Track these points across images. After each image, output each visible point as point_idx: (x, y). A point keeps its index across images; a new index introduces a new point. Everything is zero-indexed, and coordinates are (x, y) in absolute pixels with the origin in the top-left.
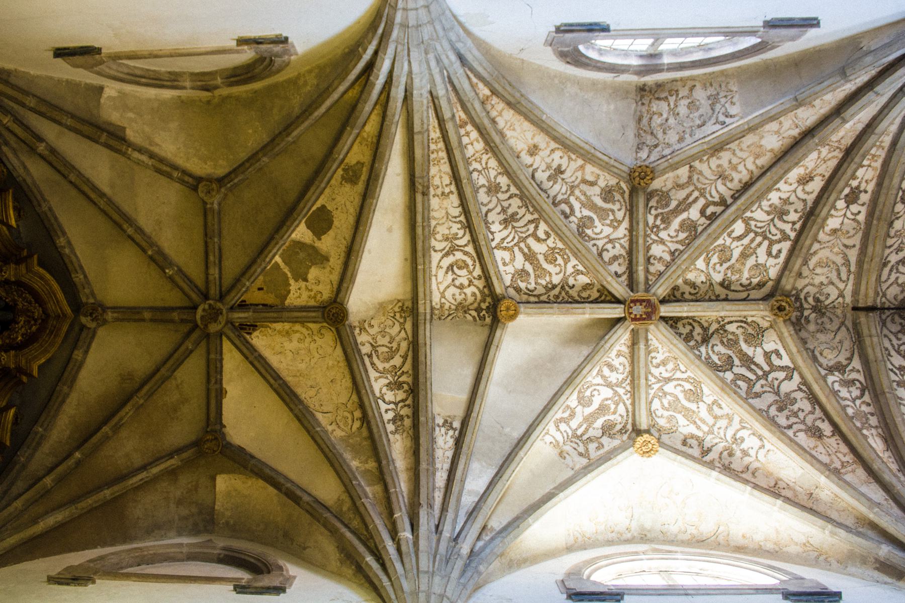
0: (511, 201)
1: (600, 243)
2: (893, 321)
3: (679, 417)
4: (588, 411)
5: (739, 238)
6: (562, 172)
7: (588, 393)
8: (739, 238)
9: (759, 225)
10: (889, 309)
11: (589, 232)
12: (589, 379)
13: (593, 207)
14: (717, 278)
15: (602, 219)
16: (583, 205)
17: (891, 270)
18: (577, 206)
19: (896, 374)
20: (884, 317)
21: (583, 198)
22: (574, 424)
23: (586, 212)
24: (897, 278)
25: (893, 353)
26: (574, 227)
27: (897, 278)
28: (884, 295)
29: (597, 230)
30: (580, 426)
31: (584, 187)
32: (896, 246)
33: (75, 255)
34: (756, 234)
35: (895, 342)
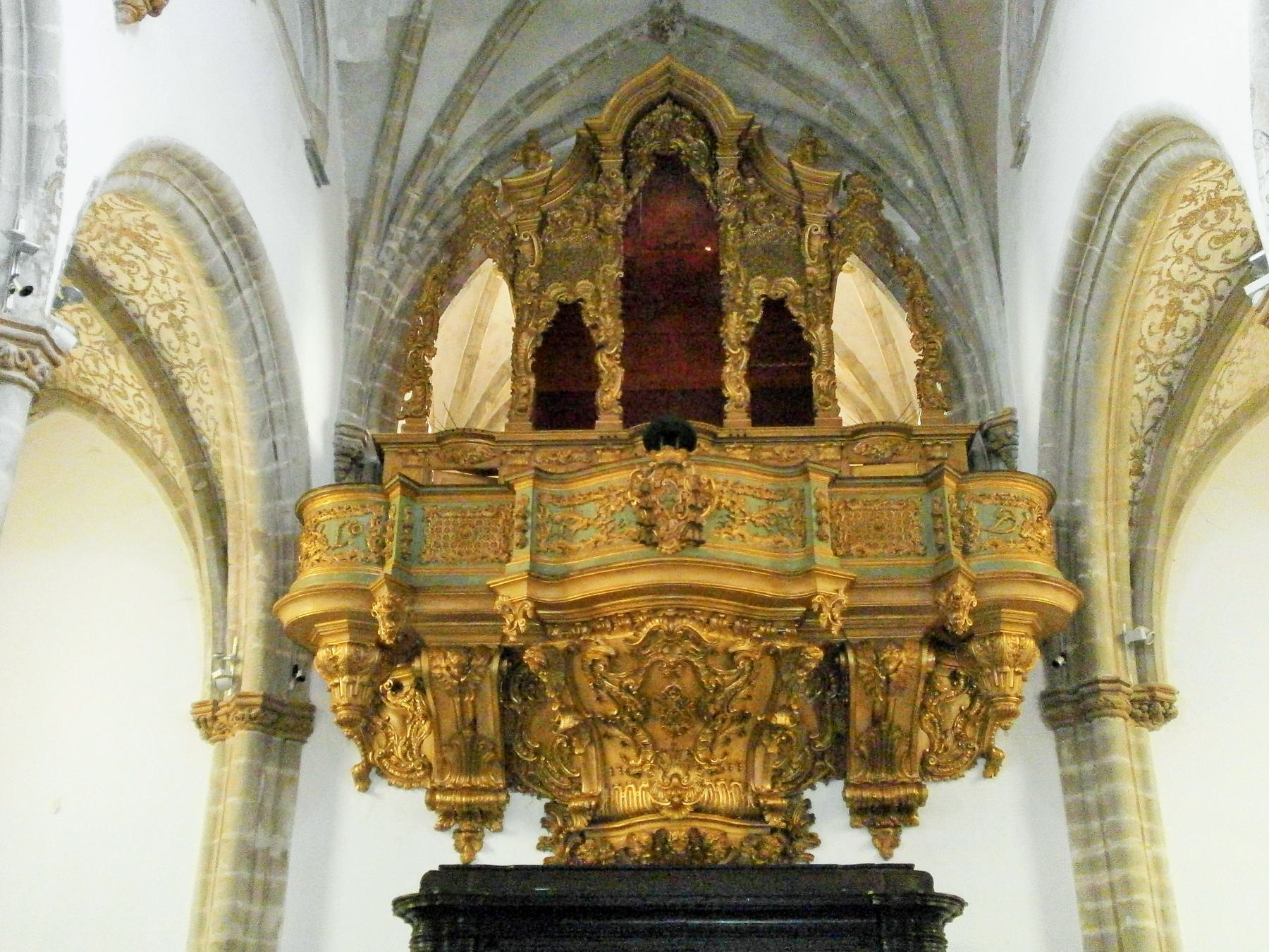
33: (580, 53)
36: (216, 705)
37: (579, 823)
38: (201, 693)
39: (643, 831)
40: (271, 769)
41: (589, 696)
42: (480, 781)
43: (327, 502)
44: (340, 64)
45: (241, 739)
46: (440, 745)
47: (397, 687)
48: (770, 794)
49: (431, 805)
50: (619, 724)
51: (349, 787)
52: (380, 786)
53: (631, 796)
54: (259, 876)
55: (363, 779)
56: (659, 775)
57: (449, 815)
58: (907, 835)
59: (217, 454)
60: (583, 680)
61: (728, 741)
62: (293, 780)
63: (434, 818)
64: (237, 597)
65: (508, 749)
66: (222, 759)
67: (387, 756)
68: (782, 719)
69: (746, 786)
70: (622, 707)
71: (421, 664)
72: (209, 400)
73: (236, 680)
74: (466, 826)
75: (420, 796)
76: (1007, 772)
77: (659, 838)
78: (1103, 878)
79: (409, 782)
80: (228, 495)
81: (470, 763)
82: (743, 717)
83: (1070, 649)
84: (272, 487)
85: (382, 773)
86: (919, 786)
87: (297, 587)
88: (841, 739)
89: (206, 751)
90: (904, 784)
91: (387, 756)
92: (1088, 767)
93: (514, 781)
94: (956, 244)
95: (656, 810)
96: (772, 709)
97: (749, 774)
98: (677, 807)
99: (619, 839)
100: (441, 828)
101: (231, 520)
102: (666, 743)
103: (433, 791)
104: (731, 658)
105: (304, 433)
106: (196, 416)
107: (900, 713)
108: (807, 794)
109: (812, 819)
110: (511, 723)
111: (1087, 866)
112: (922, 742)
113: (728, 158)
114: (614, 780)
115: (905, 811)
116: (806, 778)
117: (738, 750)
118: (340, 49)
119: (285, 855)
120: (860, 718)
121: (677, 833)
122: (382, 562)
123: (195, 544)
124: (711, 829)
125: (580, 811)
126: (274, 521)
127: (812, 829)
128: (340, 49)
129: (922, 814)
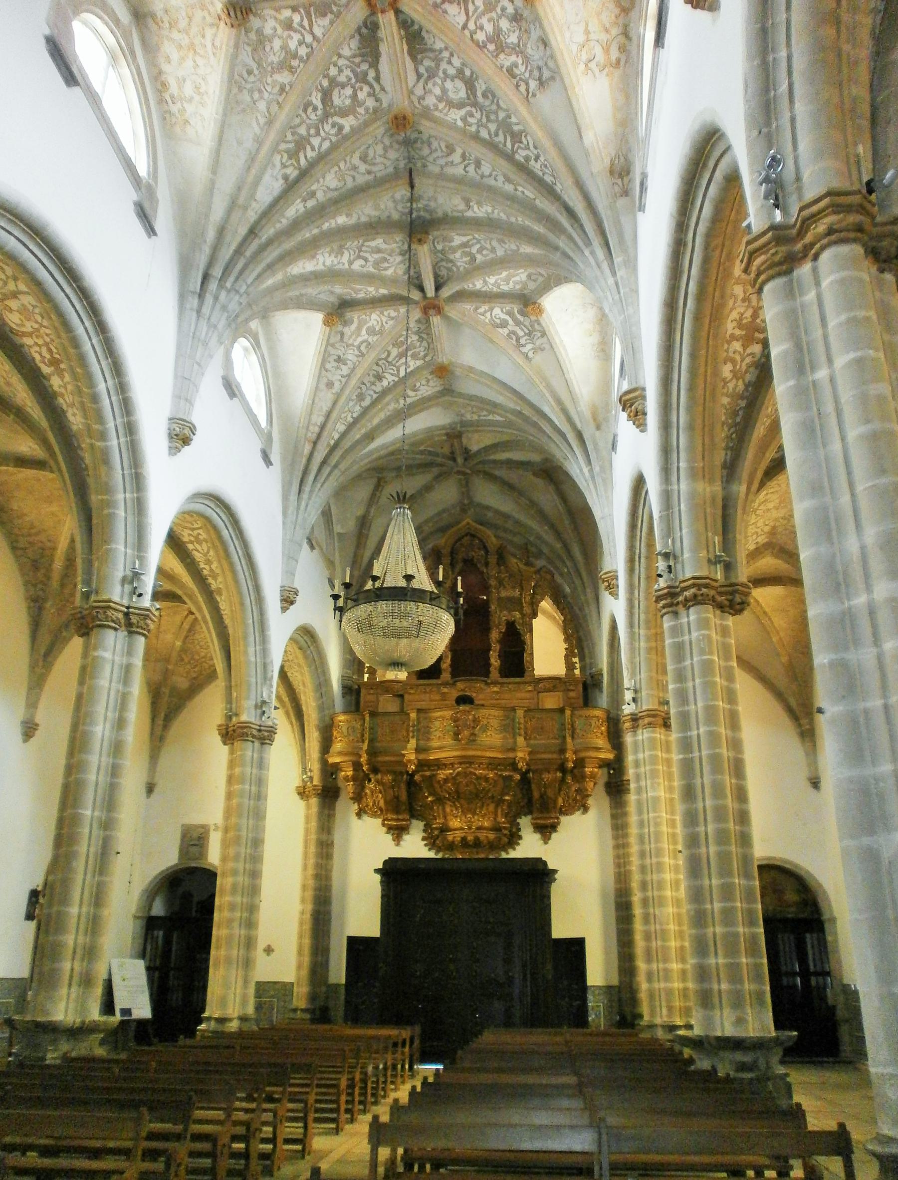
0: (366, 382)
1: (384, 319)
2: (420, 149)
3: (513, 279)
4: (511, 322)
5: (366, 260)
6: (339, 357)
7: (498, 321)
8: (366, 260)
9: (352, 253)
10: (409, 152)
11: (377, 328)
12: (487, 321)
13: (359, 329)
14: (399, 259)
15: (366, 322)
16: (359, 335)
17: (374, 164)
18: (360, 339)
19: (469, 164)
20: (417, 156)
21: (354, 337)
22: (521, 333)
23: (364, 332)
24: (380, 156)
25: (450, 159)
26: (375, 338)
27: (380, 156)
28: (397, 160)
29: (375, 323)
30: (522, 330)
31: (346, 339)
32: (352, 173)
33: (432, 517)
34: (360, 251)
35: (439, 153)
36: (304, 788)
37: (436, 833)
38: (297, 782)
39: (459, 835)
40: (326, 812)
41: (438, 790)
42: (400, 817)
43: (342, 718)
44: (339, 534)
45: (314, 801)
46: (385, 802)
47: (370, 780)
48: (504, 823)
49: (383, 825)
50: (449, 800)
51: (354, 818)
52: (366, 818)
53: (455, 823)
54: (325, 850)
55: (359, 815)
56: (463, 818)
57: (390, 829)
58: (554, 835)
59: (300, 693)
60: (436, 785)
61: (488, 805)
62: (334, 816)
63: (385, 829)
64: (310, 746)
65: (410, 804)
66: (308, 807)
67: (367, 806)
68: (507, 798)
69: (495, 819)
70: (449, 794)
71: (379, 776)
72: (296, 674)
73: (311, 778)
74: (396, 832)
75: (379, 821)
76: (592, 813)
77: (464, 839)
78: (621, 851)
79: (374, 815)
80: (304, 708)
81: (397, 810)
82: (493, 797)
83: (616, 766)
84: (321, 708)
85: (366, 813)
86: (558, 818)
87: (332, 750)
88: (530, 801)
89: (302, 804)
90: (552, 818)
91: (367, 806)
92: (619, 811)
93: (413, 816)
94: (583, 598)
95: (462, 829)
96: (503, 794)
97: (496, 815)
98: (470, 828)
99: (450, 838)
100: (387, 833)
101: (305, 717)
102: (466, 806)
103: (384, 820)
104: (486, 779)
105: (332, 687)
106: (291, 679)
107: (550, 793)
108: (519, 820)
109: (519, 830)
110: (411, 796)
111: (617, 847)
112: (560, 802)
113: (493, 560)
114: (448, 818)
115: (554, 828)
116: (518, 815)
117: (492, 807)
118: (338, 529)
119: (333, 842)
120: (536, 795)
121: (470, 838)
122: (363, 741)
123: (292, 724)
124: (482, 835)
125: (436, 828)
126: (322, 719)
127: (520, 833)
128: (338, 529)
129: (559, 828)
